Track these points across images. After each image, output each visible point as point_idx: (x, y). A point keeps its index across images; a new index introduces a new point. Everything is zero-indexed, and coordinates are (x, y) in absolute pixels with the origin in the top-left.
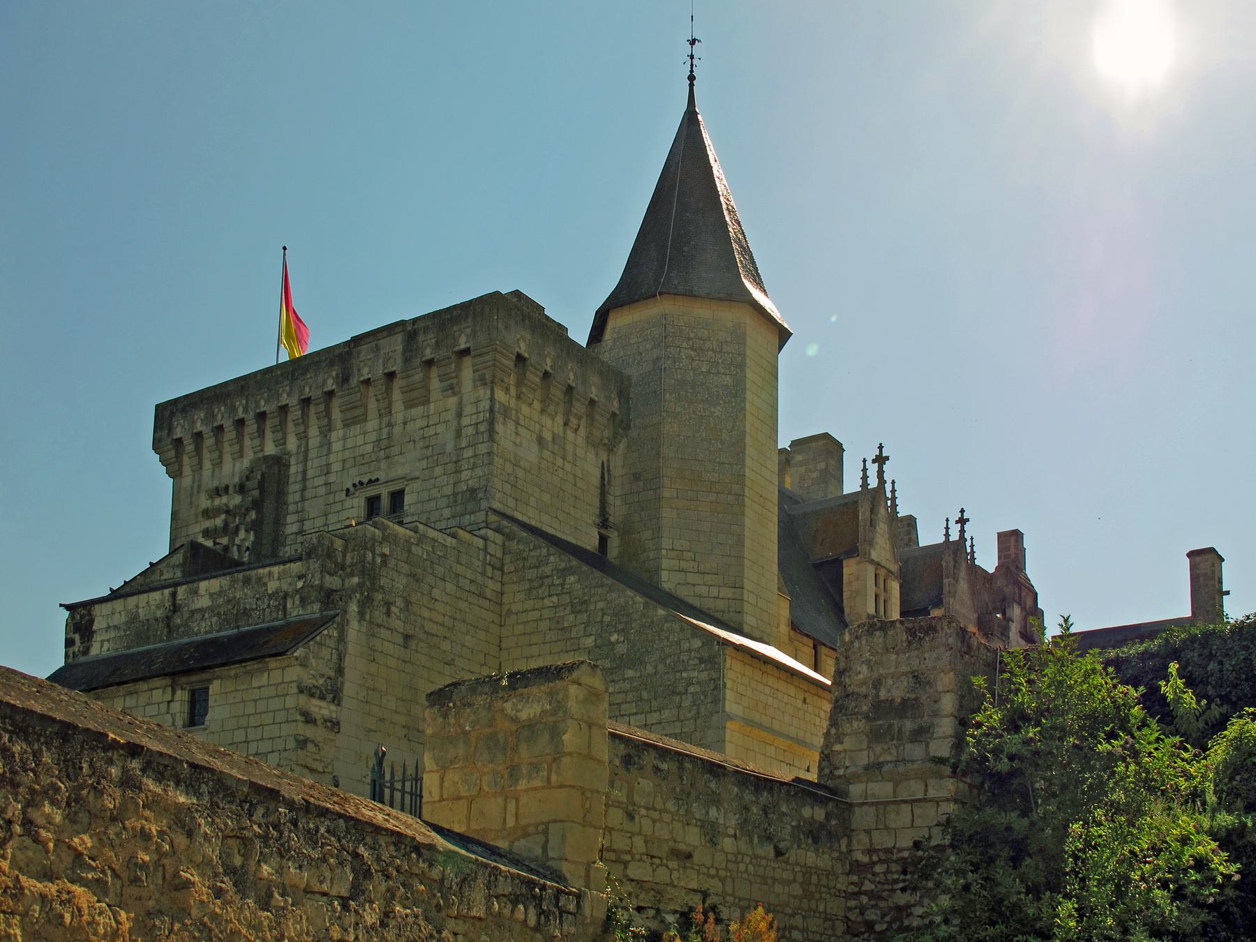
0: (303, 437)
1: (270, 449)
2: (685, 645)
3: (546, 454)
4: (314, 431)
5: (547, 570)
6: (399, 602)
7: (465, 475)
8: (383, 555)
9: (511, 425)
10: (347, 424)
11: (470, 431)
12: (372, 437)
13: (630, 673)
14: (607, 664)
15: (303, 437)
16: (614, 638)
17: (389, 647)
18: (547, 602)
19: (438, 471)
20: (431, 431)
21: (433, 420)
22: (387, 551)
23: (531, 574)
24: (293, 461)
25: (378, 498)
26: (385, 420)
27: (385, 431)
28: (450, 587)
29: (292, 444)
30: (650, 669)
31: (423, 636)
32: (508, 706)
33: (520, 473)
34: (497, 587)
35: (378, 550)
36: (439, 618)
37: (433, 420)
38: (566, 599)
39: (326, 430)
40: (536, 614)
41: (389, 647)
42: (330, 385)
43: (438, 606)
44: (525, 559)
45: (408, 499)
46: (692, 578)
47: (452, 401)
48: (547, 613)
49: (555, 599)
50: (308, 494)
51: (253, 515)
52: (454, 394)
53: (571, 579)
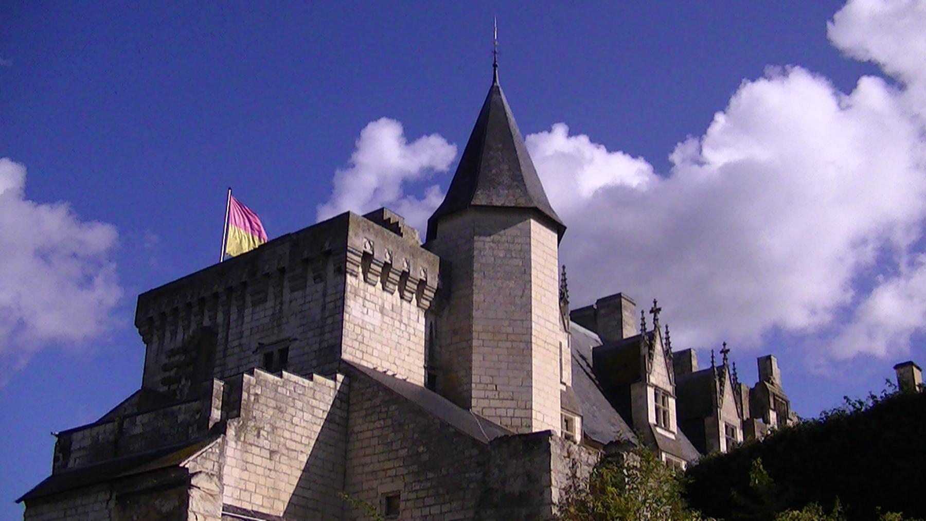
0: (227, 314)
1: (207, 322)
2: (467, 453)
3: (386, 319)
4: (234, 309)
5: (377, 401)
6: (267, 428)
7: (327, 336)
8: (256, 394)
9: (360, 300)
10: (255, 304)
11: (331, 306)
12: (270, 312)
13: (430, 475)
14: (415, 468)
16: (421, 449)
17: (258, 460)
18: (377, 424)
19: (310, 334)
20: (307, 307)
21: (308, 299)
22: (259, 392)
23: (367, 405)
24: (220, 330)
25: (272, 353)
26: (279, 300)
27: (278, 308)
28: (307, 416)
29: (220, 318)
30: (444, 472)
31: (285, 452)
32: (157, 502)
33: (366, 333)
34: (344, 414)
35: (252, 391)
36: (298, 438)
37: (308, 299)
38: (389, 422)
40: (369, 434)
41: (258, 460)
42: (244, 278)
43: (297, 429)
44: (363, 394)
45: (290, 354)
46: (495, 403)
47: (320, 287)
48: (376, 433)
49: (382, 422)
50: (229, 352)
51: (191, 368)
52: (322, 281)
53: (393, 408)
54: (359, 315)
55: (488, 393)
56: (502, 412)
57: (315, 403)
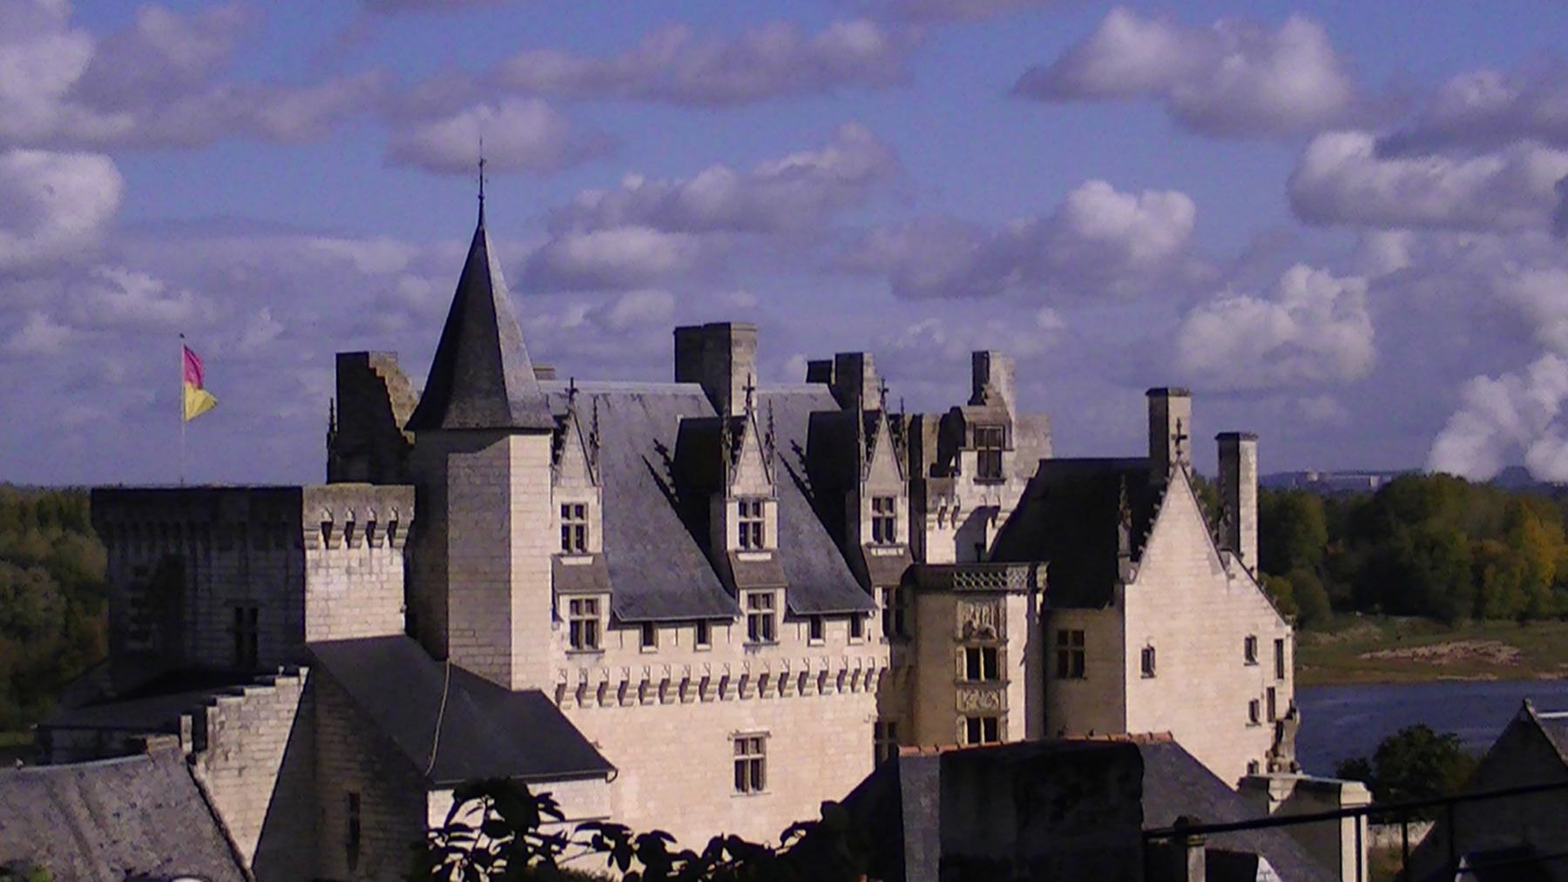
0: (193, 550)
3: (354, 578)
4: (199, 545)
15: (193, 550)
36: (264, 747)
39: (207, 550)
54: (322, 588)
55: (465, 641)
56: (480, 660)
57: (278, 707)
